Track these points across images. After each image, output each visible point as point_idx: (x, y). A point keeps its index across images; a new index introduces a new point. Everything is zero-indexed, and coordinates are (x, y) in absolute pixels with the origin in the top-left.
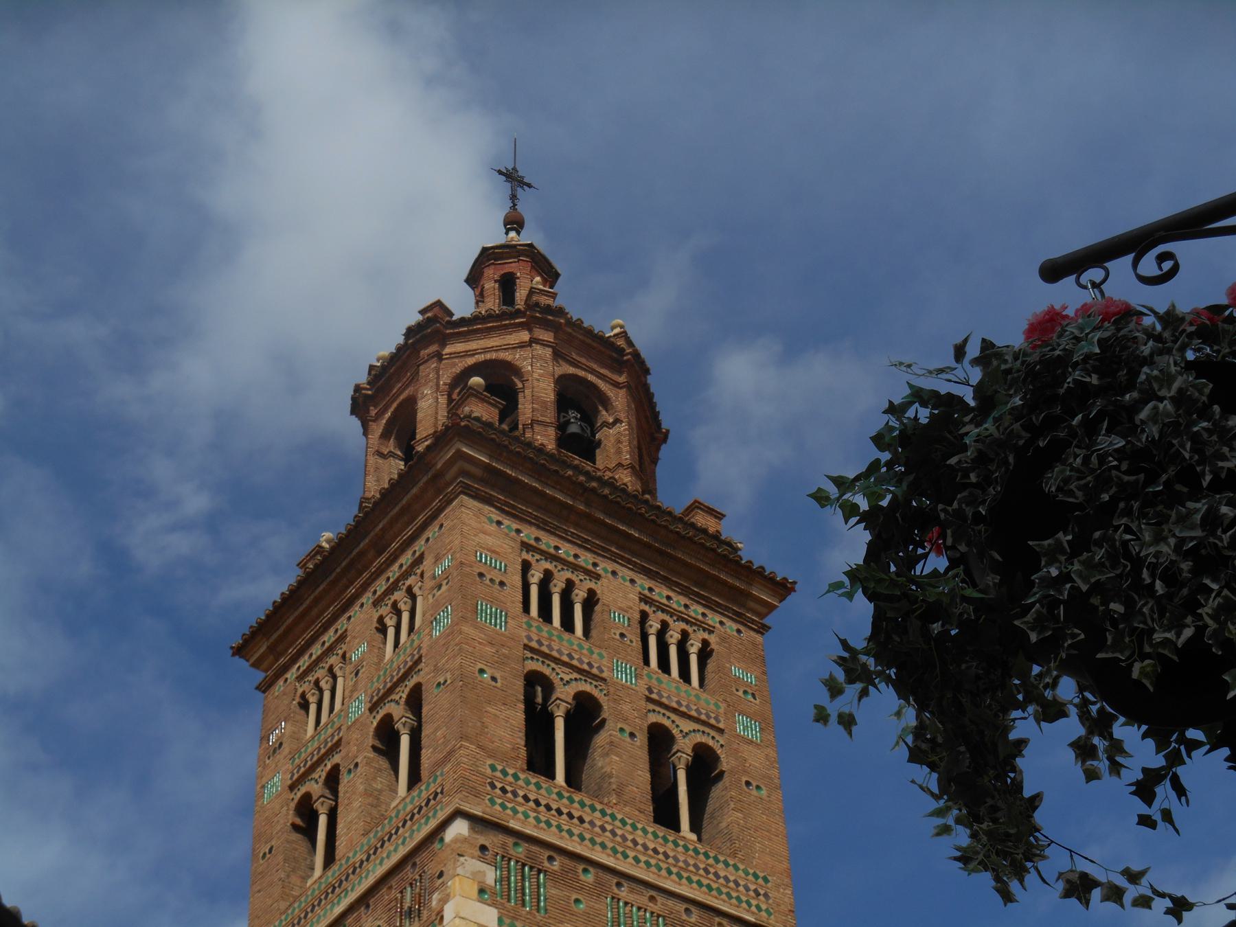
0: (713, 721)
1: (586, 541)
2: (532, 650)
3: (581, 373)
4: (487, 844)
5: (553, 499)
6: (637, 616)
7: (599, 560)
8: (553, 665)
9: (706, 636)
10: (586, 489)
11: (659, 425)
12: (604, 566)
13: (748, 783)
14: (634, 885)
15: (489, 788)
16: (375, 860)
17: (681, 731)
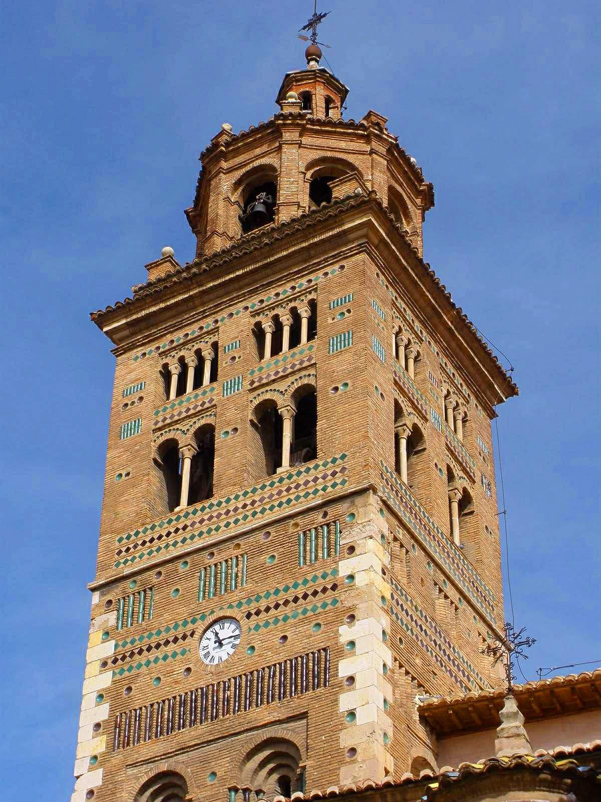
1: (204, 312)
2: (160, 429)
4: (111, 598)
5: (177, 304)
7: (219, 317)
8: (176, 427)
10: (191, 279)
12: (225, 314)
14: (222, 546)
15: (116, 556)
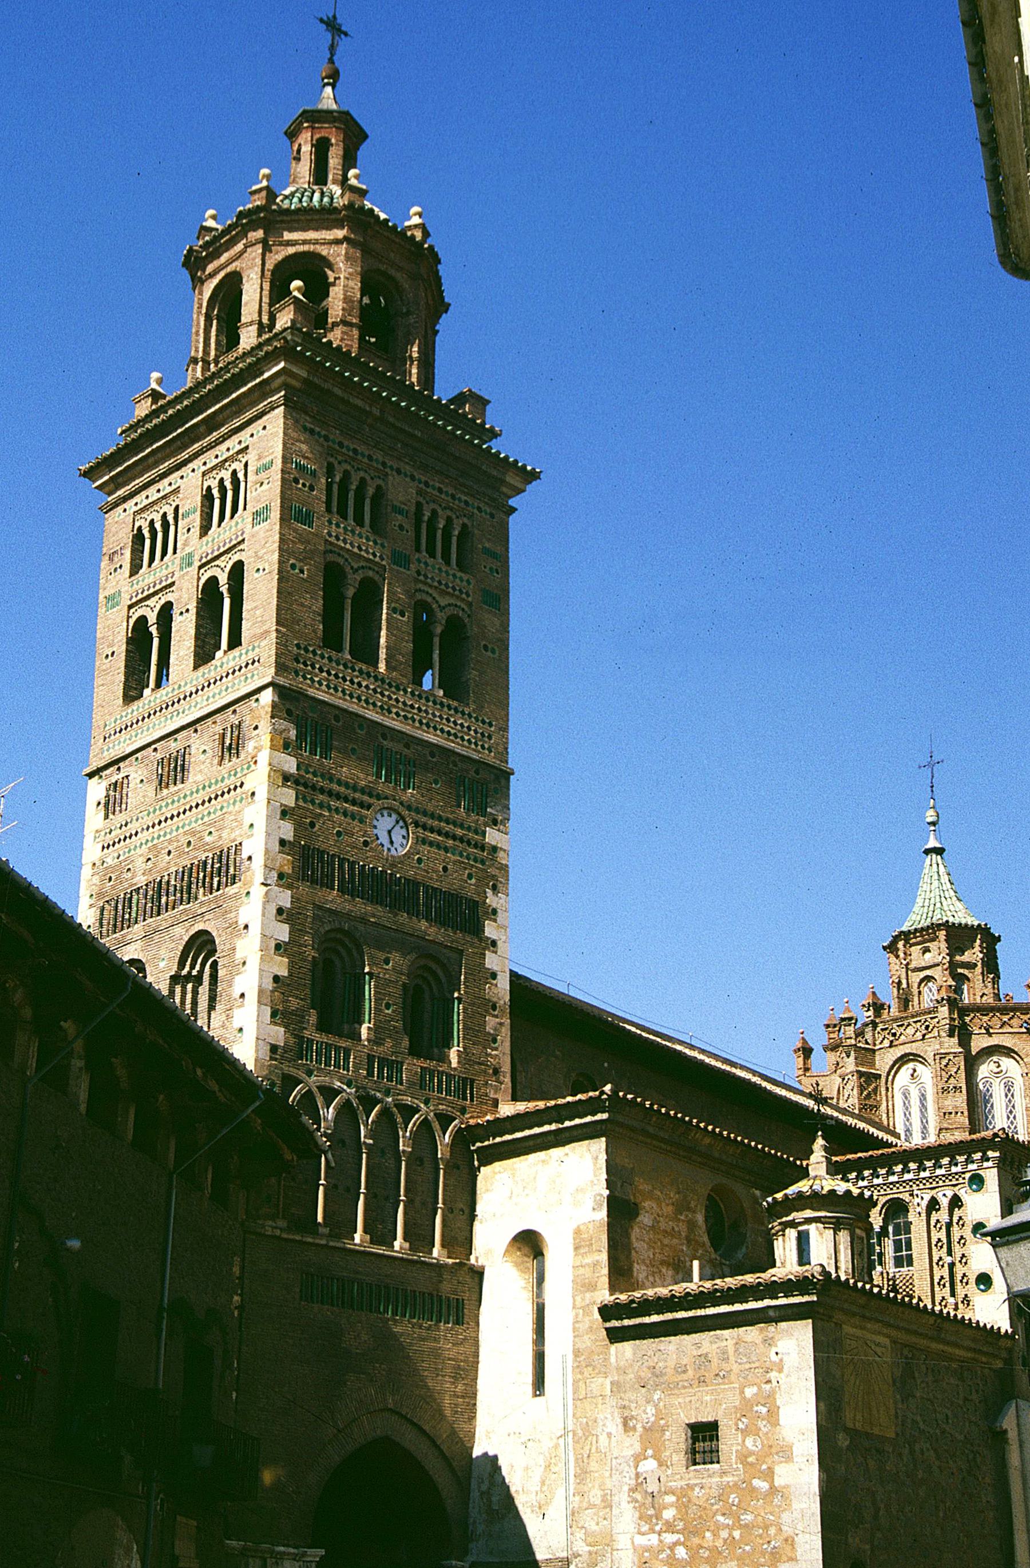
0: (464, 596)
3: (383, 267)
5: (356, 406)
6: (413, 509)
9: (466, 520)
11: (443, 298)
13: (486, 647)
16: (202, 696)
17: (440, 606)
